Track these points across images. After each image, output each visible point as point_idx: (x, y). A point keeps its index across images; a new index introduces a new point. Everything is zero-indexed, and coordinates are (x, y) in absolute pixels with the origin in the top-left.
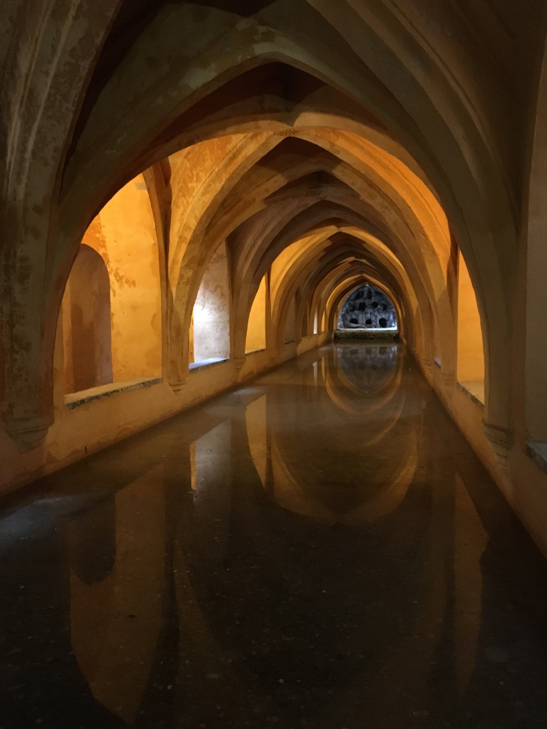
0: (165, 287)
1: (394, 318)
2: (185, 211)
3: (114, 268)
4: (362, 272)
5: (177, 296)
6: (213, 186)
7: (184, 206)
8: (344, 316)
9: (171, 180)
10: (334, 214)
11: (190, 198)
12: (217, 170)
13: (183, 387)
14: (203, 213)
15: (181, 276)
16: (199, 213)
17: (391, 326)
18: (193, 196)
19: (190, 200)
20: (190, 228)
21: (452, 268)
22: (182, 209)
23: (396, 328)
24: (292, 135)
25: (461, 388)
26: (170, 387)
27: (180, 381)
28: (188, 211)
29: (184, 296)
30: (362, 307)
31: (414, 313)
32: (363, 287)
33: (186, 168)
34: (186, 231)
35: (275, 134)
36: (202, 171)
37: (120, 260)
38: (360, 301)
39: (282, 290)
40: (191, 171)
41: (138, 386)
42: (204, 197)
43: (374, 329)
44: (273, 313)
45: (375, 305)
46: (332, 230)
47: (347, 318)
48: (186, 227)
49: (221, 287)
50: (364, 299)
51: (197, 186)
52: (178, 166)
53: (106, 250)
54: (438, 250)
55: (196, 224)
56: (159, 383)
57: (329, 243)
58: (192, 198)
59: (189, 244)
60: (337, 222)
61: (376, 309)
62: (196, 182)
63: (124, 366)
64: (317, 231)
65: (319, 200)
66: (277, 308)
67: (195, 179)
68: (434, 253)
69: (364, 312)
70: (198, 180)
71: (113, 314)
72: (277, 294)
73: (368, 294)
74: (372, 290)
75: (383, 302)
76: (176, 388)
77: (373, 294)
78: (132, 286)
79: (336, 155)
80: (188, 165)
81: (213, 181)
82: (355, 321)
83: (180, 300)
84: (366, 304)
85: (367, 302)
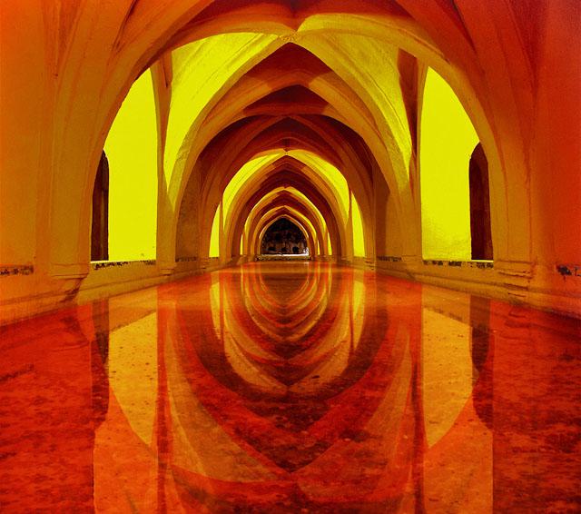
8: (263, 246)
9: (172, 83)
17: (302, 253)
23: (307, 254)
31: (345, 226)
35: (278, 39)
38: (275, 233)
45: (288, 236)
54: (403, 149)
57: (273, 168)
60: (287, 144)
82: (271, 249)
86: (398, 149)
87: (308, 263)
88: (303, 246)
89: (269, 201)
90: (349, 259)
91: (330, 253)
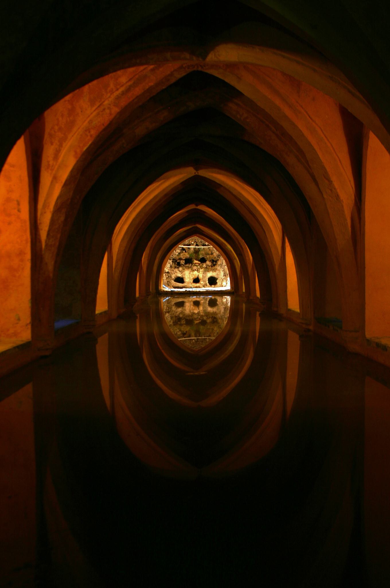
1: (225, 275)
5: (46, 245)
15: (53, 222)
24: (200, 69)
31: (277, 267)
45: (203, 260)
47: (171, 277)
54: (343, 196)
61: (204, 265)
72: (120, 245)
86: (338, 197)
87: (229, 298)
88: (222, 273)
90: (282, 311)
91: (258, 294)
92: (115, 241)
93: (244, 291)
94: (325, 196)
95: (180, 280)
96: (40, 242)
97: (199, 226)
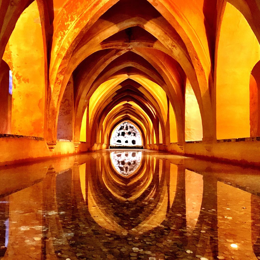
0: (47, 84)
2: (62, 39)
3: (16, 71)
4: (127, 113)
5: (54, 90)
6: (81, 23)
7: (62, 36)
10: (130, 64)
11: (66, 30)
12: (85, 12)
13: (54, 146)
14: (74, 39)
15: (57, 79)
16: (71, 40)
18: (68, 29)
19: (66, 32)
20: (65, 49)
21: (211, 77)
22: (60, 37)
25: (223, 141)
26: (47, 144)
27: (53, 142)
28: (64, 38)
29: (58, 90)
30: (123, 134)
31: (165, 124)
32: (123, 124)
33: (64, 14)
34: (62, 51)
36: (75, 14)
37: (20, 66)
38: (122, 131)
39: (95, 110)
40: (67, 16)
41: (33, 138)
42: (75, 29)
43: (130, 145)
44: (90, 123)
45: (129, 133)
46: (124, 77)
48: (62, 48)
49: (68, 100)
50: (124, 130)
51: (71, 23)
52: (59, 12)
53: (11, 60)
54: (204, 68)
55: (69, 46)
56: (42, 140)
57: (120, 87)
58: (67, 31)
59: (63, 59)
60: (128, 71)
61: (130, 135)
62: (71, 21)
63: (19, 131)
64: (118, 76)
65: (128, 51)
66: (92, 120)
67: (70, 19)
68: (202, 69)
69: (124, 137)
70: (72, 19)
71: (14, 99)
73: (126, 128)
74: (128, 126)
75: (134, 132)
76: (50, 146)
77: (128, 128)
78: (27, 83)
79: (154, 7)
80: (65, 12)
81: (82, 19)
82: (119, 141)
83: (55, 93)
84: (125, 133)
85: (126, 132)
89: (118, 111)
92: (90, 111)
93: (148, 144)
94: (195, 68)
95: (119, 141)
96: (50, 88)
97: (128, 115)
